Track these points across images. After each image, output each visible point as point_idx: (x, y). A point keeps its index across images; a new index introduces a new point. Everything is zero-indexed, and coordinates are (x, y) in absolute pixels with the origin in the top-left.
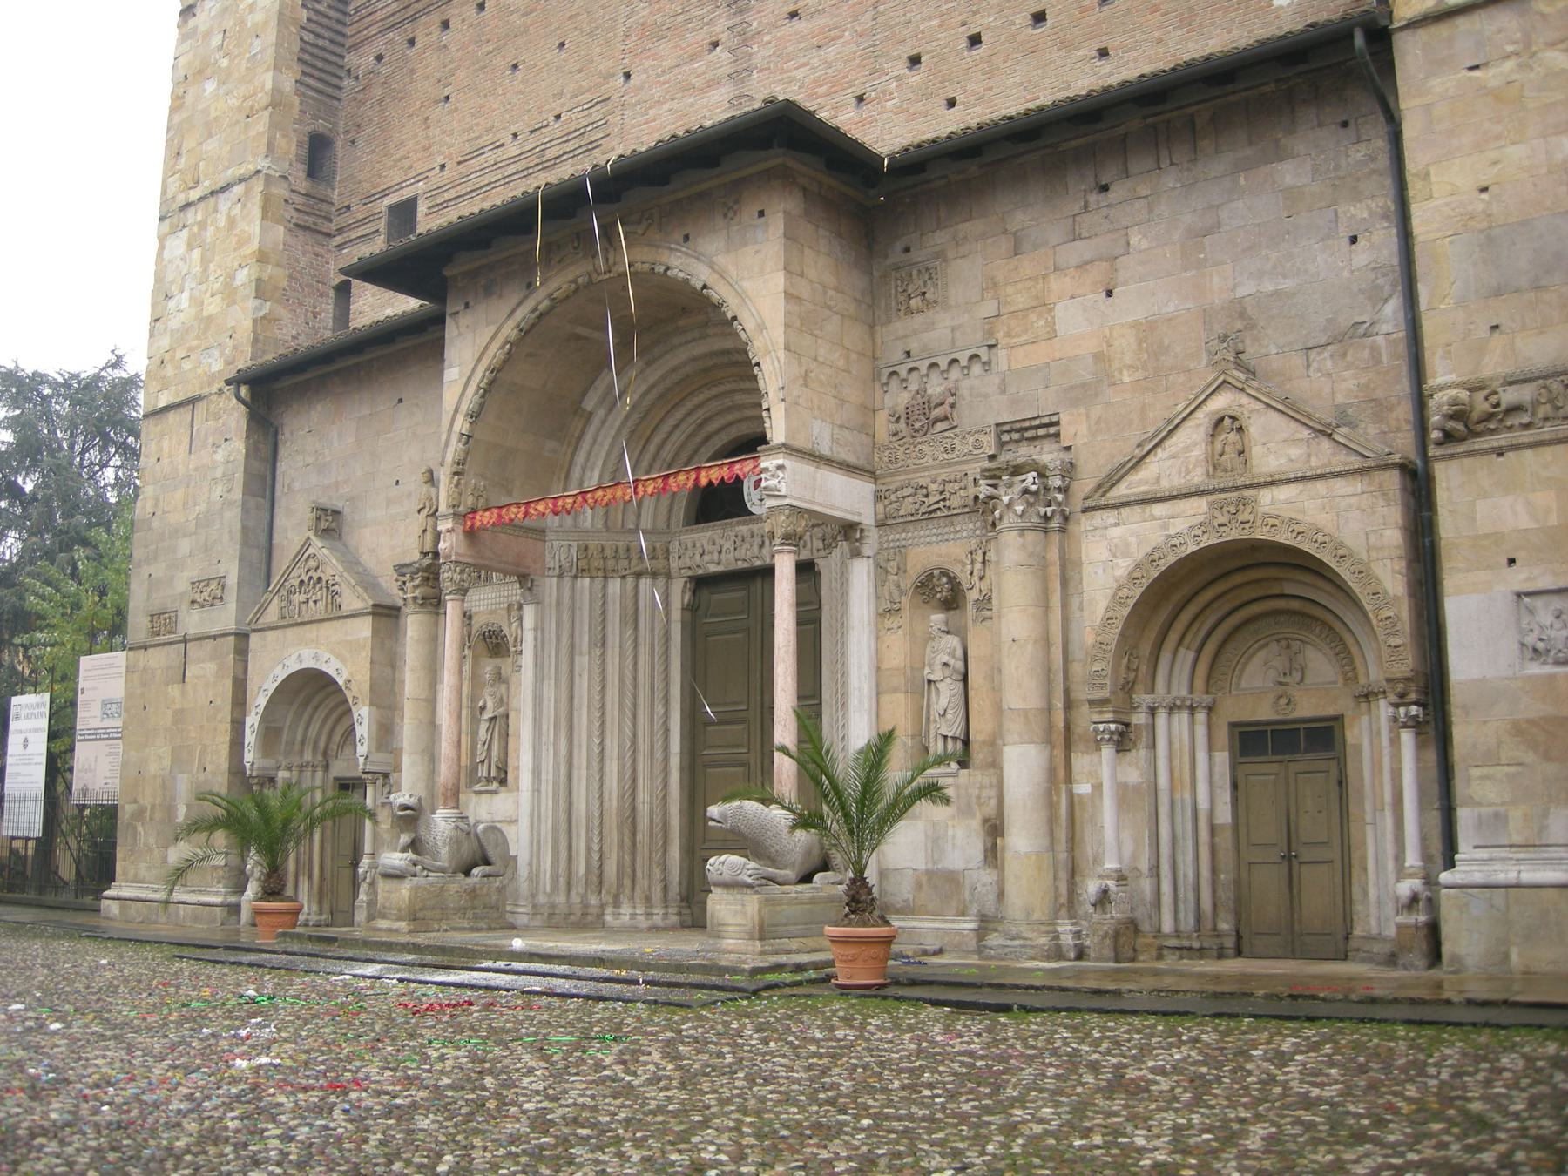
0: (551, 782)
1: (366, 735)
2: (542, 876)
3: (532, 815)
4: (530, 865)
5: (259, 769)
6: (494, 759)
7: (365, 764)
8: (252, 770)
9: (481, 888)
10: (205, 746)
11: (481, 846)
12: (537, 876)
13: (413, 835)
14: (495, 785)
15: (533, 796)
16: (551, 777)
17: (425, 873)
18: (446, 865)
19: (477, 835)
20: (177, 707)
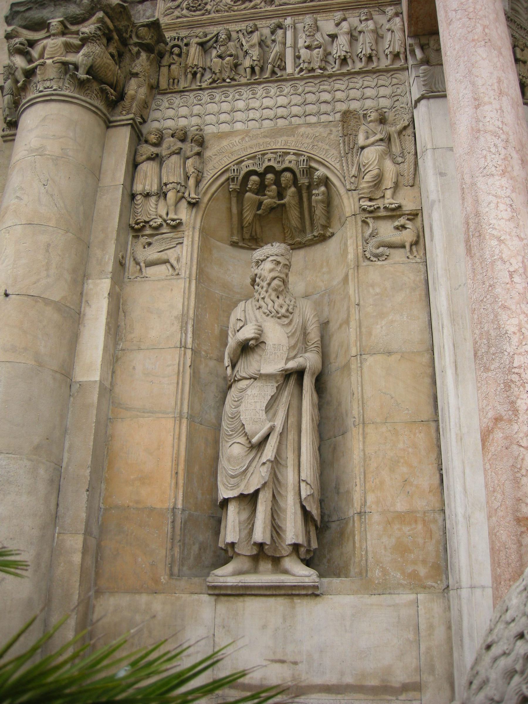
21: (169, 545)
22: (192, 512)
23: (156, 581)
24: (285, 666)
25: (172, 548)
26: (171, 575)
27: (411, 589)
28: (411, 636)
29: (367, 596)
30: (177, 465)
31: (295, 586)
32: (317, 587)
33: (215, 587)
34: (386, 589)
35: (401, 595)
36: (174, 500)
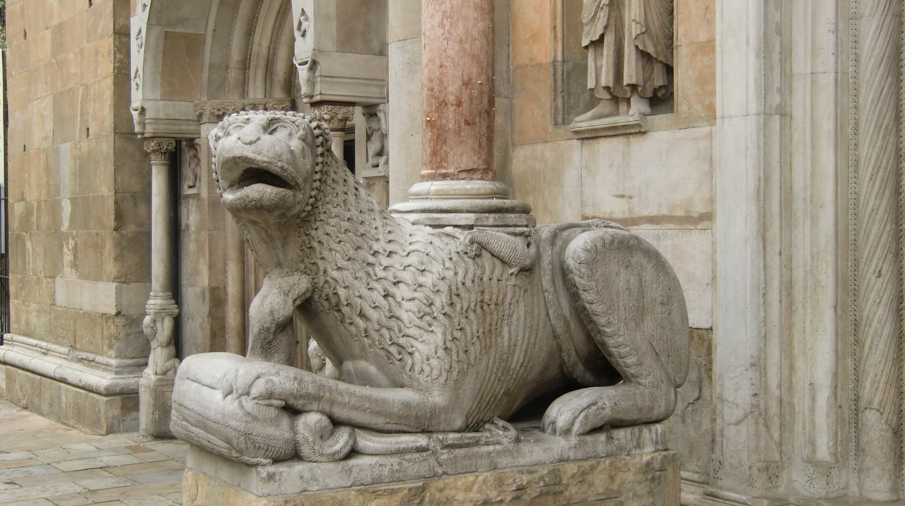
0: (827, 81)
1: (310, 12)
2: (801, 403)
3: (762, 196)
4: (759, 365)
5: (156, 120)
6: (632, 30)
7: (311, 82)
8: (143, 124)
9: (582, 477)
10: (86, 87)
11: (582, 315)
12: (786, 405)
13: (302, 284)
14: (638, 107)
15: (764, 129)
16: (827, 61)
17: (341, 440)
18: (438, 398)
19: (564, 272)
20: (55, 22)
21: (553, 97)
22: (578, 62)
23: (546, 131)
24: (624, 200)
25: (555, 99)
26: (556, 124)
27: (708, 121)
28: (706, 168)
29: (677, 131)
30: (555, 19)
31: (624, 126)
32: (639, 125)
33: (576, 132)
34: (690, 123)
35: (701, 128)
36: (553, 54)
